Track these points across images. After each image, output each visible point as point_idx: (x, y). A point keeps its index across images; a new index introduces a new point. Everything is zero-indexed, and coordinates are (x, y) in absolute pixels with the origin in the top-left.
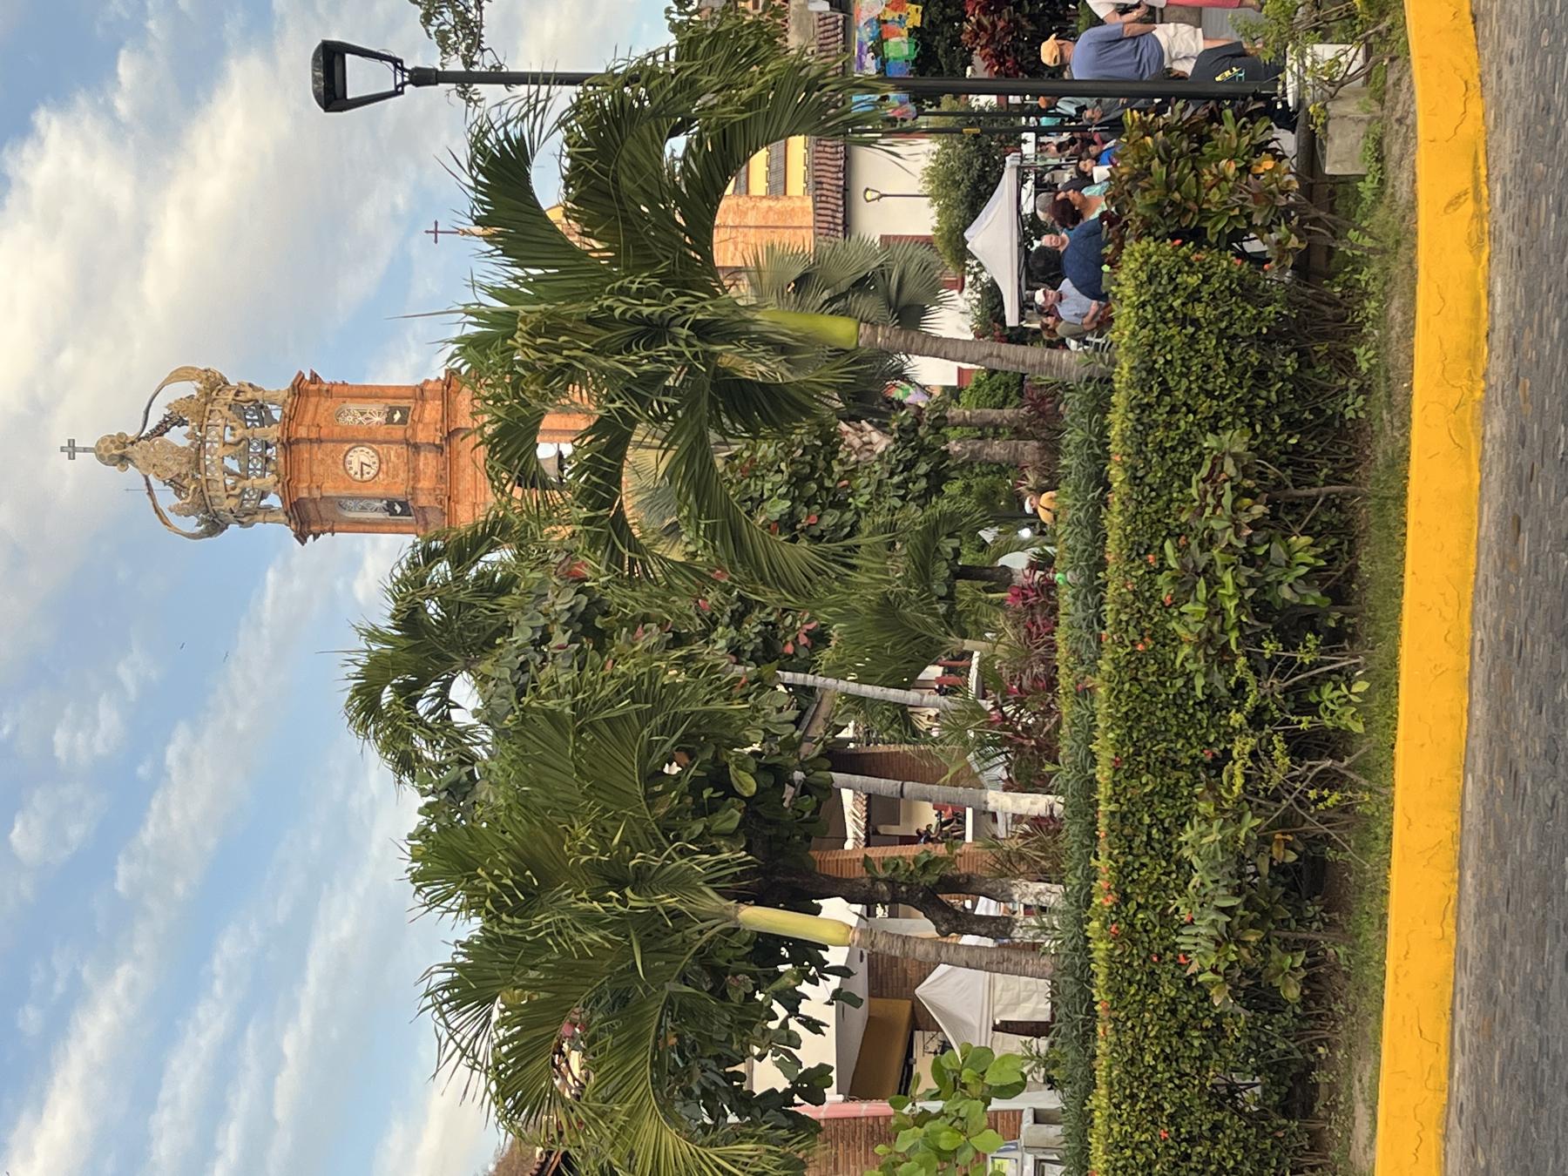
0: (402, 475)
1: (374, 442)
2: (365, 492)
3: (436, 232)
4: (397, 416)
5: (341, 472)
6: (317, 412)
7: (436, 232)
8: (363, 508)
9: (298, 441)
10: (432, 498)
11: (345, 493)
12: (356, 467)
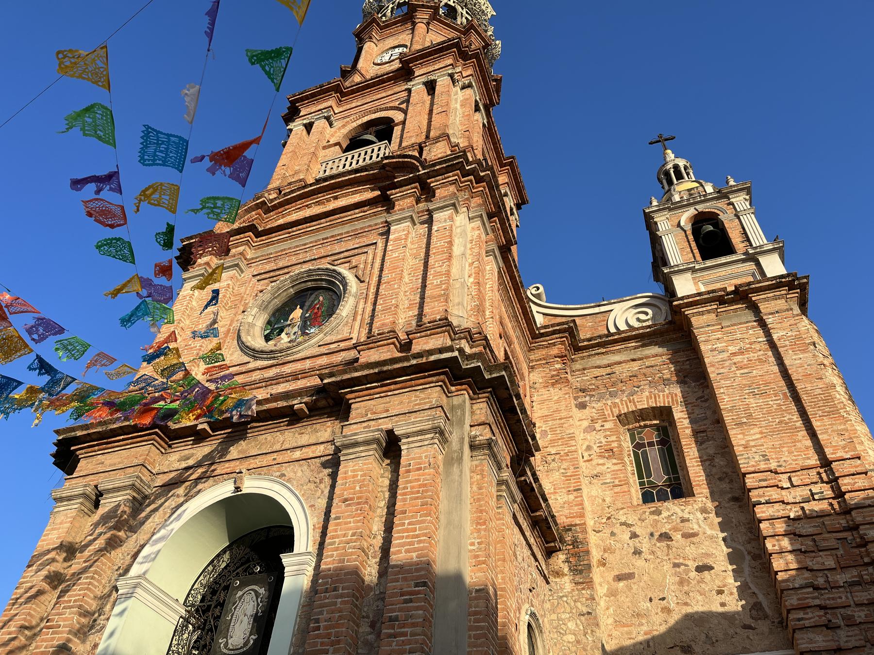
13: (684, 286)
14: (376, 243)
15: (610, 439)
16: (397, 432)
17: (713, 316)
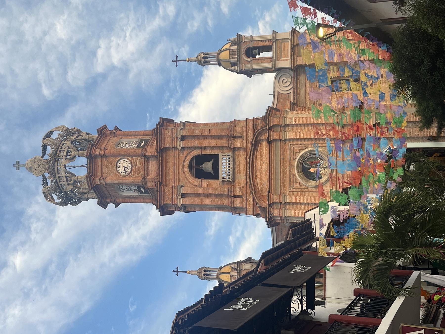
0: (142, 173)
1: (129, 156)
2: (124, 181)
3: (177, 61)
4: (143, 144)
5: (115, 172)
6: (109, 145)
7: (177, 61)
8: (129, 191)
9: (96, 156)
10: (154, 184)
11: (116, 182)
12: (122, 169)
13: (285, 63)
14: (290, 145)
15: (335, 97)
16: (374, 123)
17: (298, 58)
